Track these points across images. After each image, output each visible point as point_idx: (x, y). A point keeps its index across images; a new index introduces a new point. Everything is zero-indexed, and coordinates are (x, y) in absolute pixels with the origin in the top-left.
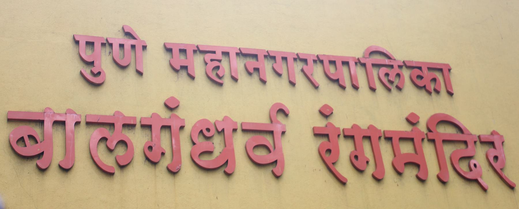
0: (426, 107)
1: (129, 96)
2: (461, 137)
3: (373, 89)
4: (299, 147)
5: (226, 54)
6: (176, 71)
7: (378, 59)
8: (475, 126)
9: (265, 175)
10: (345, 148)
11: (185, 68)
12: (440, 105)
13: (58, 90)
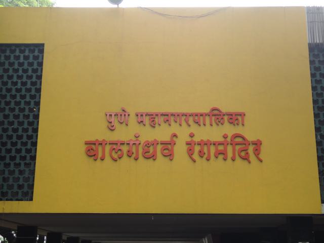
0: (229, 130)
1: (123, 134)
2: (245, 142)
3: (211, 125)
4: (180, 149)
5: (157, 115)
6: (139, 123)
7: (216, 112)
8: (250, 138)
9: (167, 159)
10: (197, 148)
11: (142, 122)
12: (238, 130)
13: (100, 133)
